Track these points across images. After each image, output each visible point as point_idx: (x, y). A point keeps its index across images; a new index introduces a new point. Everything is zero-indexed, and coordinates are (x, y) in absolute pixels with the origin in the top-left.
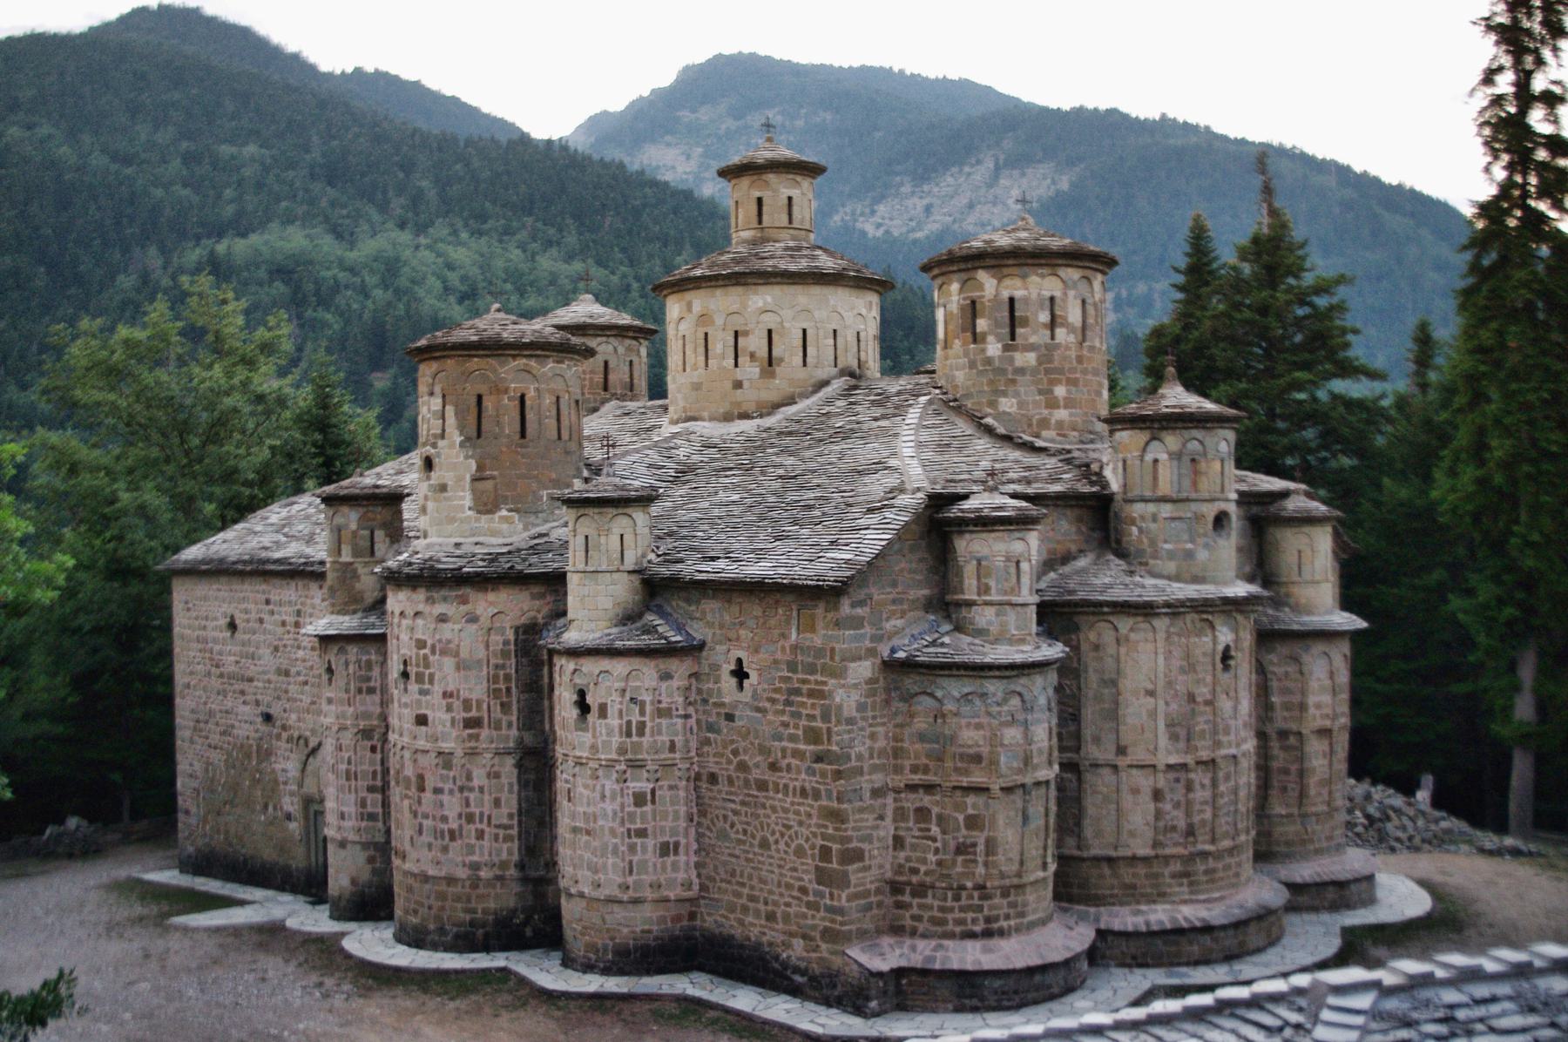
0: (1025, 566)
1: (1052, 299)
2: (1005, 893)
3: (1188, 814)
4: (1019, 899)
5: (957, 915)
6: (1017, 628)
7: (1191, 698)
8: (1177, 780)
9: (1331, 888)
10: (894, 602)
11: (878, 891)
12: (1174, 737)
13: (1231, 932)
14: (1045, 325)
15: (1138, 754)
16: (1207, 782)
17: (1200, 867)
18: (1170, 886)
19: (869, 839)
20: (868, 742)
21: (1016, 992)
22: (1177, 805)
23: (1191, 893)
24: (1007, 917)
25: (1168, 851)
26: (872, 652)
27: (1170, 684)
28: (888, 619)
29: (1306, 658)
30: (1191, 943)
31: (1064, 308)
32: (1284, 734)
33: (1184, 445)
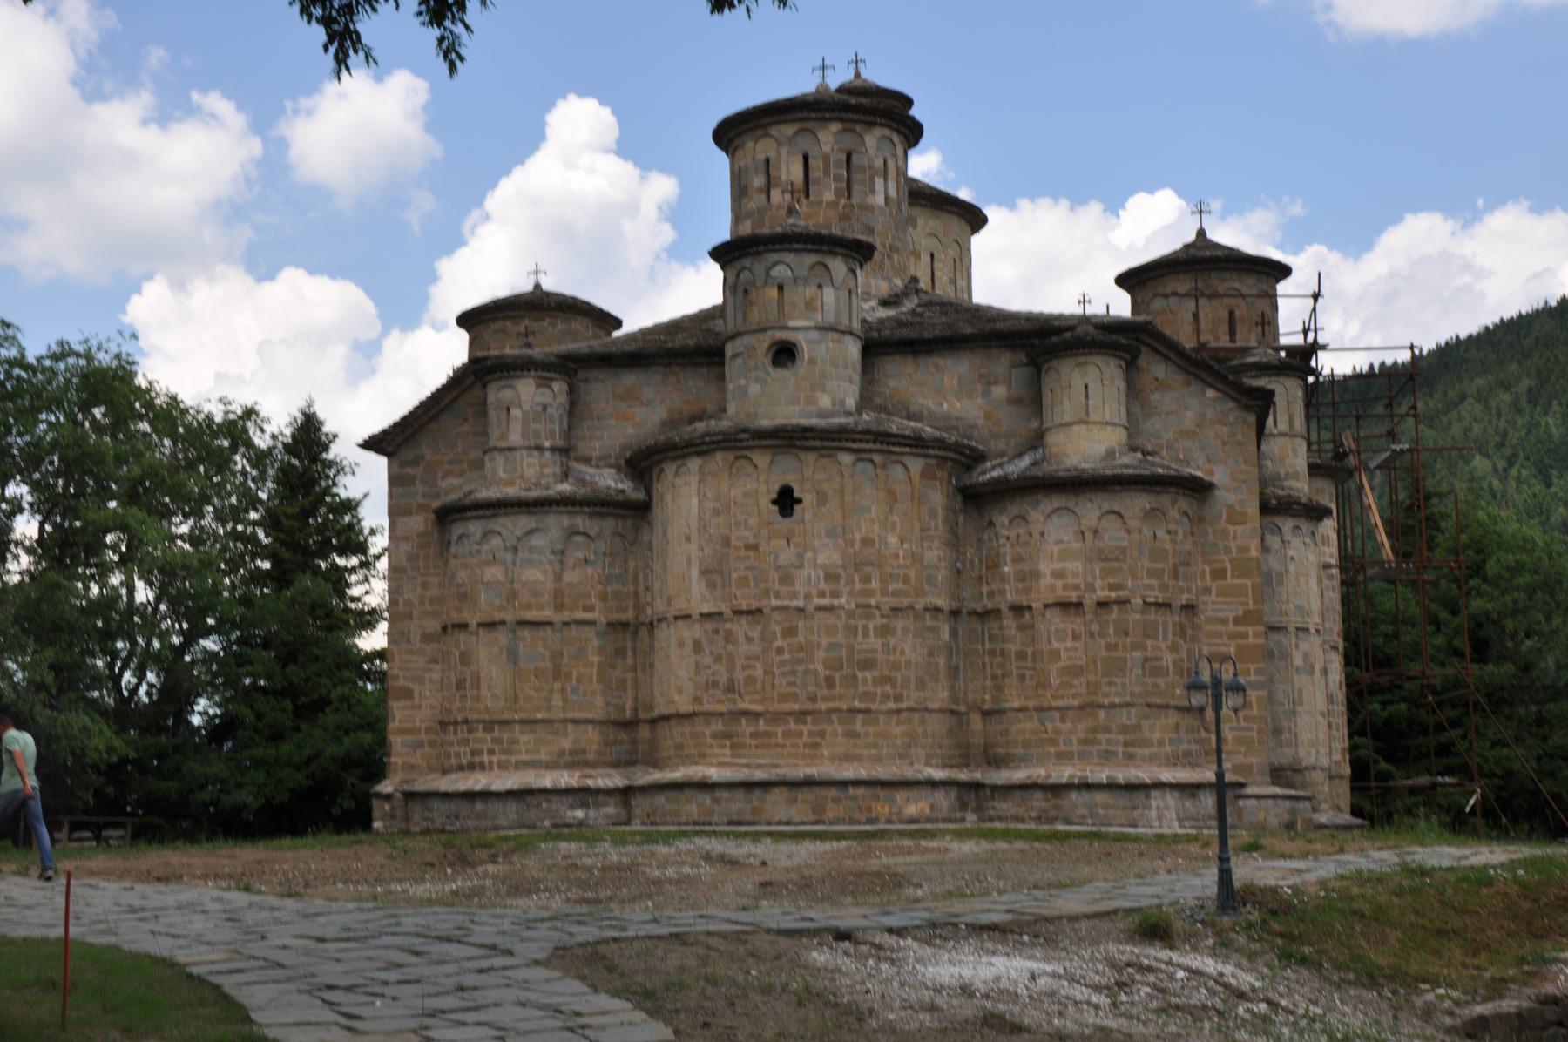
0: (515, 412)
1: (768, 161)
2: (489, 726)
3: (731, 668)
4: (506, 736)
5: (456, 748)
6: (505, 471)
7: (726, 542)
8: (716, 631)
9: (1039, 794)
10: (450, 462)
11: (428, 730)
12: (711, 585)
13: (740, 794)
14: (760, 190)
15: (680, 605)
16: (755, 634)
17: (745, 727)
18: (711, 746)
19: (421, 680)
20: (419, 590)
21: (457, 817)
22: (718, 659)
23: (734, 756)
24: (491, 752)
25: (707, 707)
26: (422, 508)
27: (703, 528)
28: (444, 478)
29: (1035, 515)
30: (690, 802)
31: (778, 168)
32: (1018, 609)
33: (738, 276)
